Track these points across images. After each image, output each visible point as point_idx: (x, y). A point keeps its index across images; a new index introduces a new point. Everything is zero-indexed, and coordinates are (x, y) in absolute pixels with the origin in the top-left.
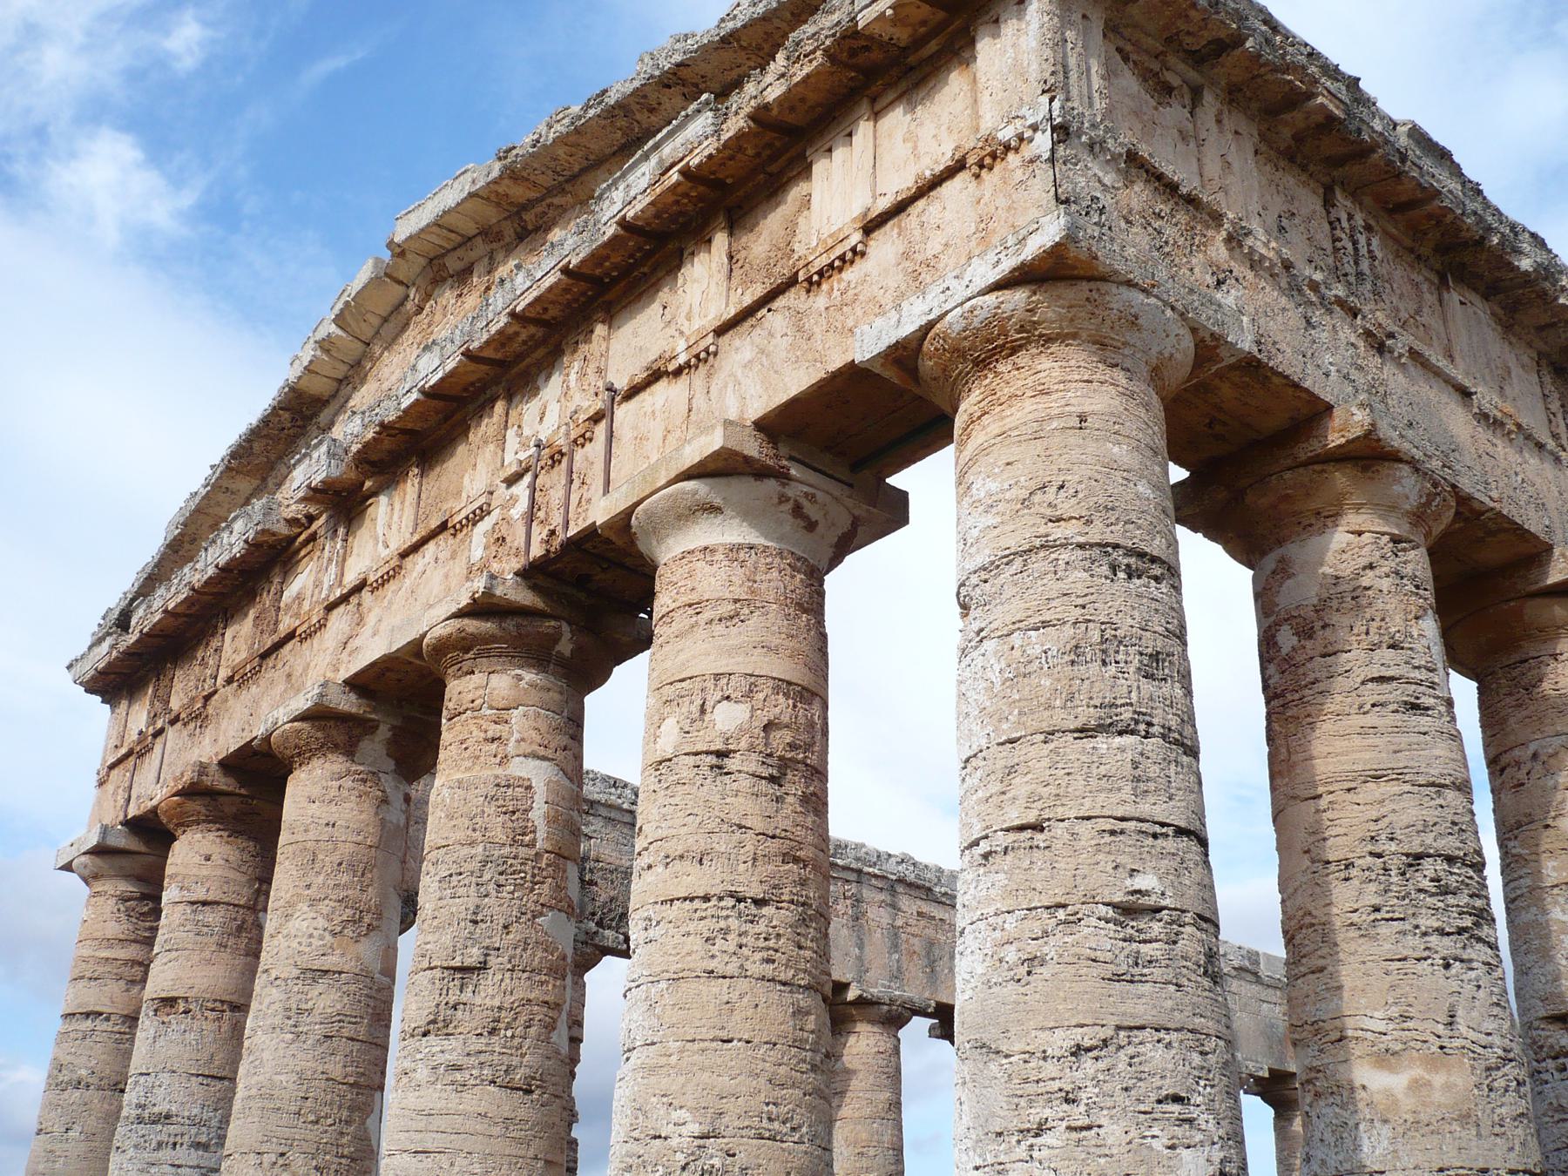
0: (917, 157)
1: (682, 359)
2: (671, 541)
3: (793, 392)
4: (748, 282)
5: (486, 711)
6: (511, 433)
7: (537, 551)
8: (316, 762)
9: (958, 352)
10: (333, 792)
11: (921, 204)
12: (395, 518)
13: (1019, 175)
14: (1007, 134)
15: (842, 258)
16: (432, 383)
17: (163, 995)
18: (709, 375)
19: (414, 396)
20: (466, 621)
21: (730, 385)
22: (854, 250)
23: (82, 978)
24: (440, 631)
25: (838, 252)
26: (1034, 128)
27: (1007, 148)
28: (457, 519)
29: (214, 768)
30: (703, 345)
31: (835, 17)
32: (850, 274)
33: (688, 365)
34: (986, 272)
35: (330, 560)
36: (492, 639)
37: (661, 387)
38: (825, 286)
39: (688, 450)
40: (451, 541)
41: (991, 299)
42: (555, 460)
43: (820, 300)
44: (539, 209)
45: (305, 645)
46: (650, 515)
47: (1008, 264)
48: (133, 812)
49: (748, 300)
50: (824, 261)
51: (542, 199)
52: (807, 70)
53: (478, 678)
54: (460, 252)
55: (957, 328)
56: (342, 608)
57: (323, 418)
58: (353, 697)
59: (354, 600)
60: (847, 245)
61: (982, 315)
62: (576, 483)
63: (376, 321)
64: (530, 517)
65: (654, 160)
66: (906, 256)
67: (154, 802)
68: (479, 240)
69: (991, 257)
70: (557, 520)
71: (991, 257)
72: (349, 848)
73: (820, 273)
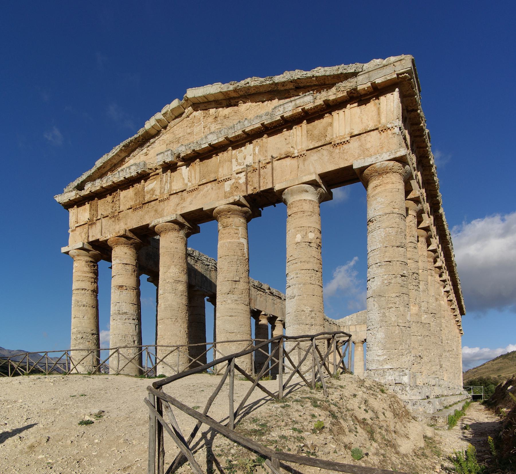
0: (362, 123)
1: (296, 155)
2: (295, 197)
3: (330, 170)
4: (312, 139)
5: (234, 227)
6: (234, 160)
7: (250, 192)
8: (170, 233)
10: (176, 241)
11: (365, 135)
12: (193, 175)
13: (391, 136)
14: (389, 126)
15: (344, 142)
18: (304, 160)
20: (231, 205)
21: (311, 164)
22: (347, 141)
25: (343, 140)
26: (396, 126)
27: (389, 129)
28: (220, 180)
29: (127, 231)
30: (303, 153)
32: (345, 146)
33: (298, 156)
34: (387, 156)
35: (166, 182)
36: (236, 211)
37: (288, 159)
38: (338, 147)
39: (304, 178)
40: (217, 185)
41: (387, 162)
42: (254, 170)
43: (337, 150)
45: (161, 203)
46: (292, 190)
47: (392, 157)
49: (317, 145)
50: (339, 141)
53: (231, 219)
54: (206, 105)
55: (378, 166)
56: (175, 195)
58: (182, 218)
59: (180, 194)
60: (346, 140)
61: (385, 165)
64: (247, 183)
66: (361, 146)
68: (213, 103)
69: (388, 153)
70: (256, 185)
71: (388, 153)
72: (181, 254)
73: (338, 144)
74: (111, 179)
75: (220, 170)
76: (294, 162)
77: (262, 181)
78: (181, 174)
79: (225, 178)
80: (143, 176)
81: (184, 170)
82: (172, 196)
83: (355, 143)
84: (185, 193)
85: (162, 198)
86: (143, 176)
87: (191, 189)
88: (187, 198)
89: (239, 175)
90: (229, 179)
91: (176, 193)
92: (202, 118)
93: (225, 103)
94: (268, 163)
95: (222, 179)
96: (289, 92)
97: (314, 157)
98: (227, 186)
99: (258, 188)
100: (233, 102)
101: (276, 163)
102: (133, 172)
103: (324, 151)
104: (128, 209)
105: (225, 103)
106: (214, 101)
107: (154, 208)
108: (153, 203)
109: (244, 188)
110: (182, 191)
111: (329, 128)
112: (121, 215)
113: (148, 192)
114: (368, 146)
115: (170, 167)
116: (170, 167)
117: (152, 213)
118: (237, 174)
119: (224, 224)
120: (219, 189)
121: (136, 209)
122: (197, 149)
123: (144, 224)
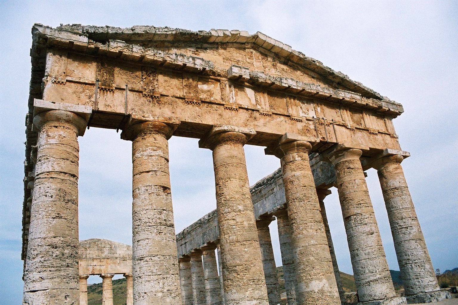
9: (396, 159)
16: (294, 87)
17: (165, 186)
19: (287, 86)
23: (68, 160)
24: (305, 142)
28: (293, 117)
30: (353, 128)
31: (380, 103)
33: (350, 129)
43: (372, 136)
44: (294, 64)
48: (101, 108)
51: (296, 63)
52: (375, 106)
56: (245, 111)
57: (205, 45)
59: (250, 112)
62: (327, 132)
63: (235, 41)
65: (350, 94)
67: (147, 119)
74: (162, 56)
75: (290, 109)
76: (348, 131)
77: (328, 135)
78: (246, 95)
79: (298, 118)
80: (203, 75)
81: (250, 92)
82: (241, 110)
83: (379, 137)
84: (256, 114)
85: (230, 107)
86: (203, 75)
87: (265, 113)
88: (260, 119)
89: (309, 122)
90: (301, 121)
91: (247, 109)
92: (260, 58)
93: (283, 60)
94: (331, 124)
95: (296, 118)
96: (333, 83)
97: (359, 134)
98: (300, 126)
99: (326, 138)
100: (290, 63)
101: (335, 126)
102: (199, 65)
103: (365, 133)
104: (177, 97)
105: (283, 60)
106: (275, 53)
107: (220, 112)
108: (215, 106)
109: (314, 133)
110: (253, 110)
111: (362, 121)
112: (165, 99)
113: (203, 91)
114: (387, 142)
115: (238, 83)
116: (238, 83)
117: (217, 116)
118: (307, 120)
119: (303, 157)
120: (292, 124)
121: (191, 103)
122: (277, 83)
123: (204, 122)
